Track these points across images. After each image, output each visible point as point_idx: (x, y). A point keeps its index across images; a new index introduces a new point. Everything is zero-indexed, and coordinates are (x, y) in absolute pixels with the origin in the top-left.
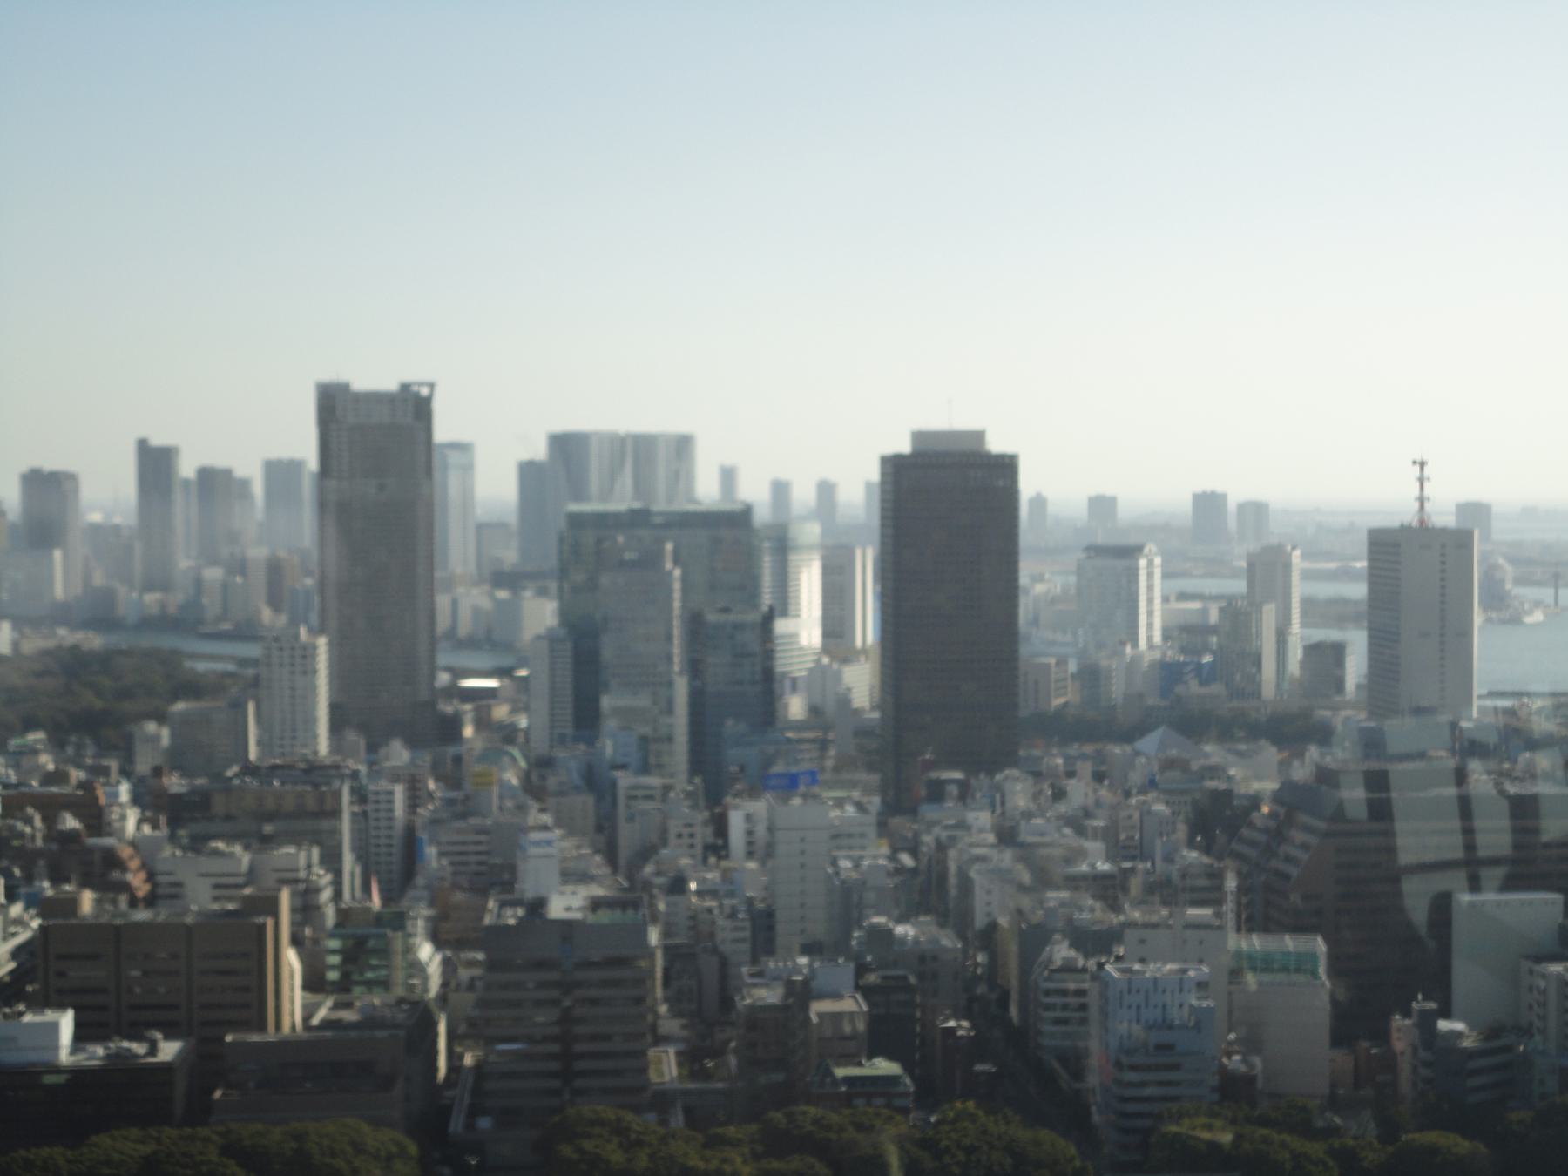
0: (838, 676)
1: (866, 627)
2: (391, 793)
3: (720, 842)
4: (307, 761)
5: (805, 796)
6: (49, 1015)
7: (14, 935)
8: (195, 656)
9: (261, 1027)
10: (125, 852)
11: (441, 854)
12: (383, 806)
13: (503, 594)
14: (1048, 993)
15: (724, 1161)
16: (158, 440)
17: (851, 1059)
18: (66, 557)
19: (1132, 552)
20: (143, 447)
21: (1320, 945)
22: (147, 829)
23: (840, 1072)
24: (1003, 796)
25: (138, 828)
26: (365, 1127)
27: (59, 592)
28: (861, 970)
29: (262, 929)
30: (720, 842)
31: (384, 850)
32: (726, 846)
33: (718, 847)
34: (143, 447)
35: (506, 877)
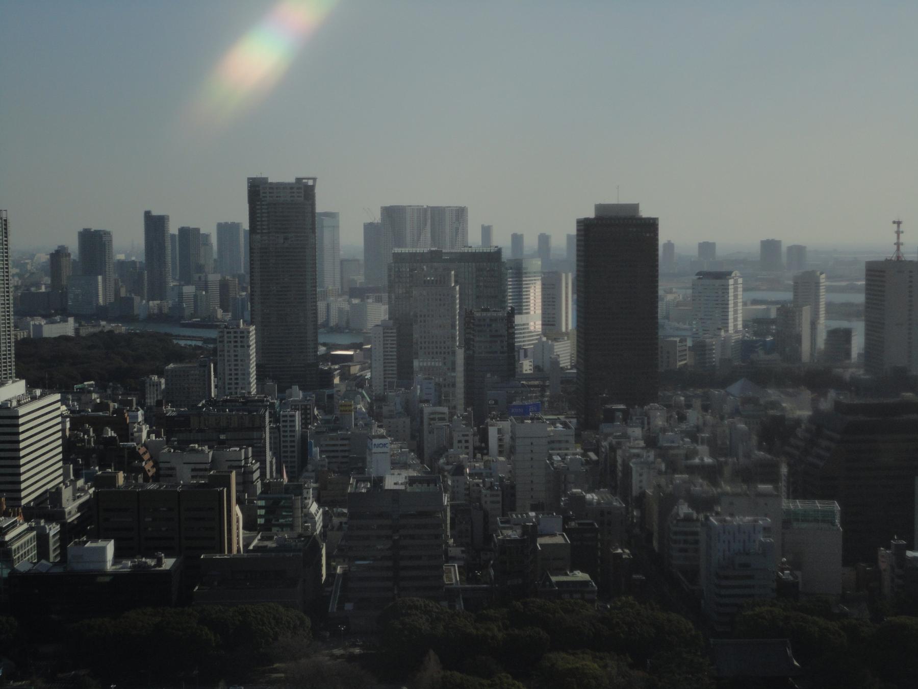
0: (552, 347)
1: (568, 319)
2: (293, 416)
3: (483, 445)
4: (244, 397)
5: (532, 419)
6: (100, 543)
7: (79, 497)
8: (178, 337)
9: (222, 551)
10: (142, 450)
11: (321, 452)
12: (288, 424)
13: (356, 301)
14: (676, 533)
16: (155, 212)
17: (561, 571)
18: (104, 280)
19: (723, 276)
20: (148, 215)
21: (837, 506)
22: (153, 437)
23: (554, 579)
24: (649, 418)
25: (148, 436)
26: (281, 609)
27: (101, 301)
28: (566, 520)
30: (483, 445)
31: (289, 449)
32: (487, 447)
33: (482, 448)
34: (148, 215)
35: (360, 465)
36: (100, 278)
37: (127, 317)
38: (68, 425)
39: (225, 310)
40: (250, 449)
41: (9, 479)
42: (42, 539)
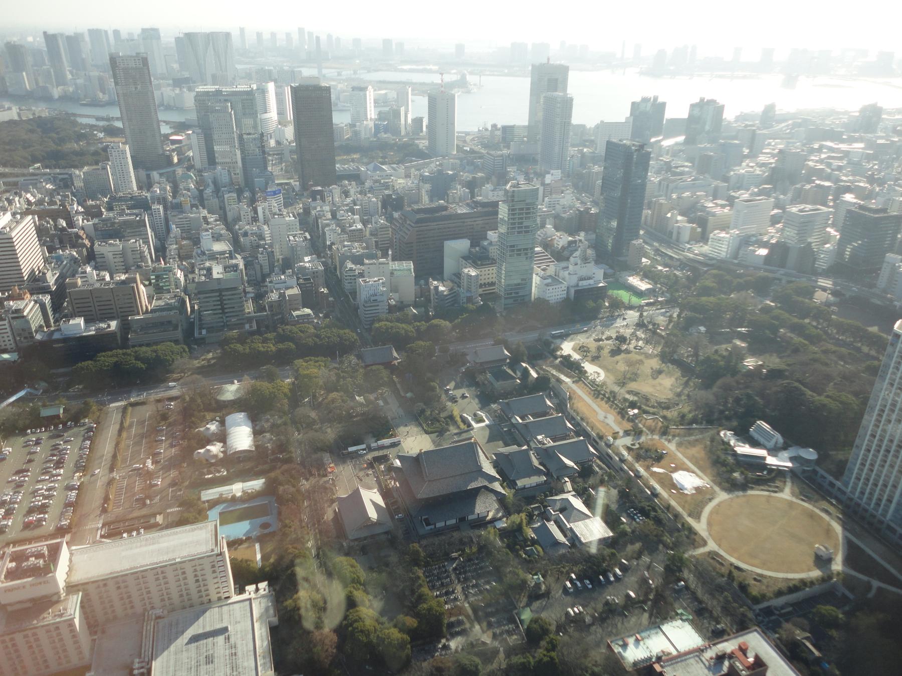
0: (283, 131)
1: (290, 115)
7: (55, 274)
10: (81, 233)
11: (177, 228)
15: (268, 347)
16: (51, 31)
17: (298, 309)
18: (27, 75)
19: (363, 89)
20: (45, 33)
21: (411, 265)
22: (85, 221)
28: (298, 279)
29: (133, 287)
32: (258, 217)
33: (255, 219)
36: (24, 73)
37: (47, 98)
38: (37, 219)
39: (104, 93)
40: (141, 241)
41: (18, 276)
42: (43, 307)
